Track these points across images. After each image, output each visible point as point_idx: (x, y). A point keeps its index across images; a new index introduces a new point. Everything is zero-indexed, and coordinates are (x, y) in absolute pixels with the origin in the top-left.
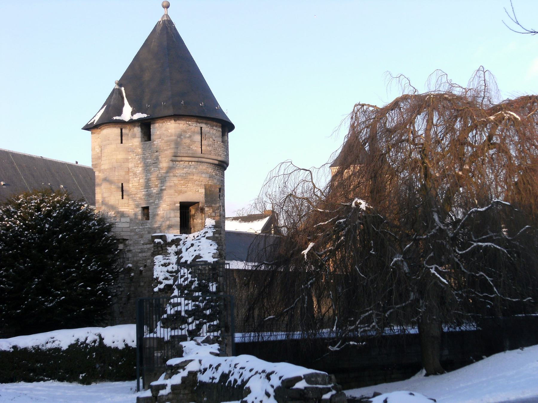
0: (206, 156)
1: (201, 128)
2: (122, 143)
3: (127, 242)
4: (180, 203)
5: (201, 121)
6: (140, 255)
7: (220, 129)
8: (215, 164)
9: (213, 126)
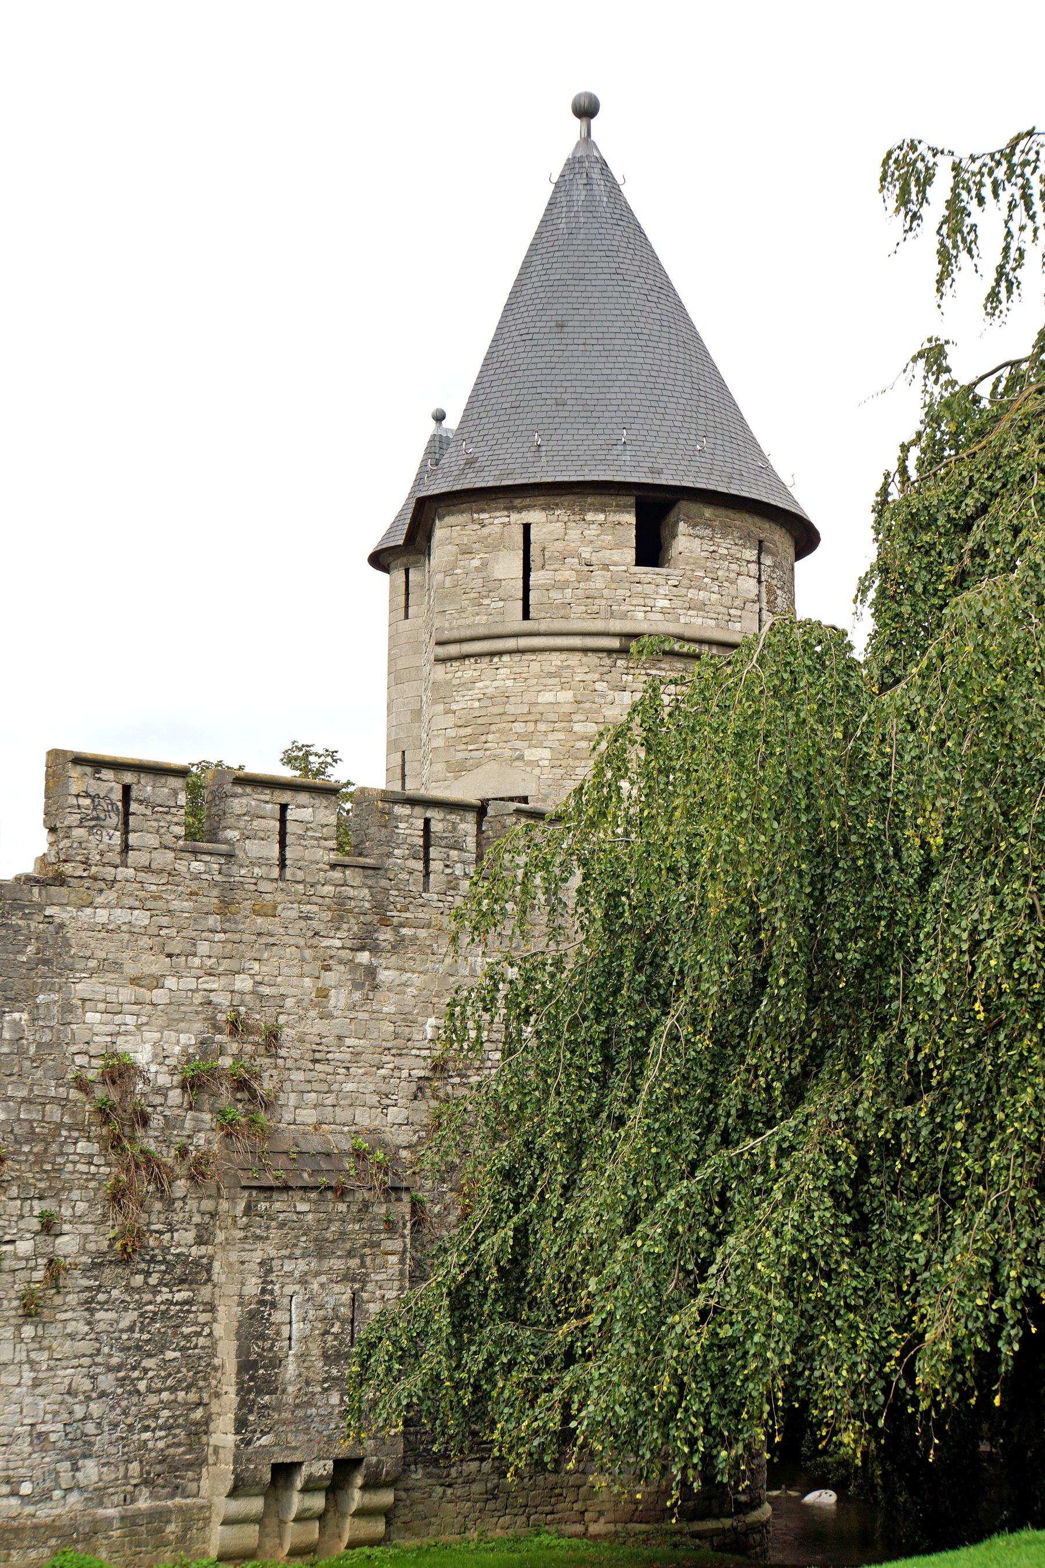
0: (543, 626)
1: (527, 527)
2: (407, 617)
5: (527, 501)
8: (610, 652)
9: (583, 511)
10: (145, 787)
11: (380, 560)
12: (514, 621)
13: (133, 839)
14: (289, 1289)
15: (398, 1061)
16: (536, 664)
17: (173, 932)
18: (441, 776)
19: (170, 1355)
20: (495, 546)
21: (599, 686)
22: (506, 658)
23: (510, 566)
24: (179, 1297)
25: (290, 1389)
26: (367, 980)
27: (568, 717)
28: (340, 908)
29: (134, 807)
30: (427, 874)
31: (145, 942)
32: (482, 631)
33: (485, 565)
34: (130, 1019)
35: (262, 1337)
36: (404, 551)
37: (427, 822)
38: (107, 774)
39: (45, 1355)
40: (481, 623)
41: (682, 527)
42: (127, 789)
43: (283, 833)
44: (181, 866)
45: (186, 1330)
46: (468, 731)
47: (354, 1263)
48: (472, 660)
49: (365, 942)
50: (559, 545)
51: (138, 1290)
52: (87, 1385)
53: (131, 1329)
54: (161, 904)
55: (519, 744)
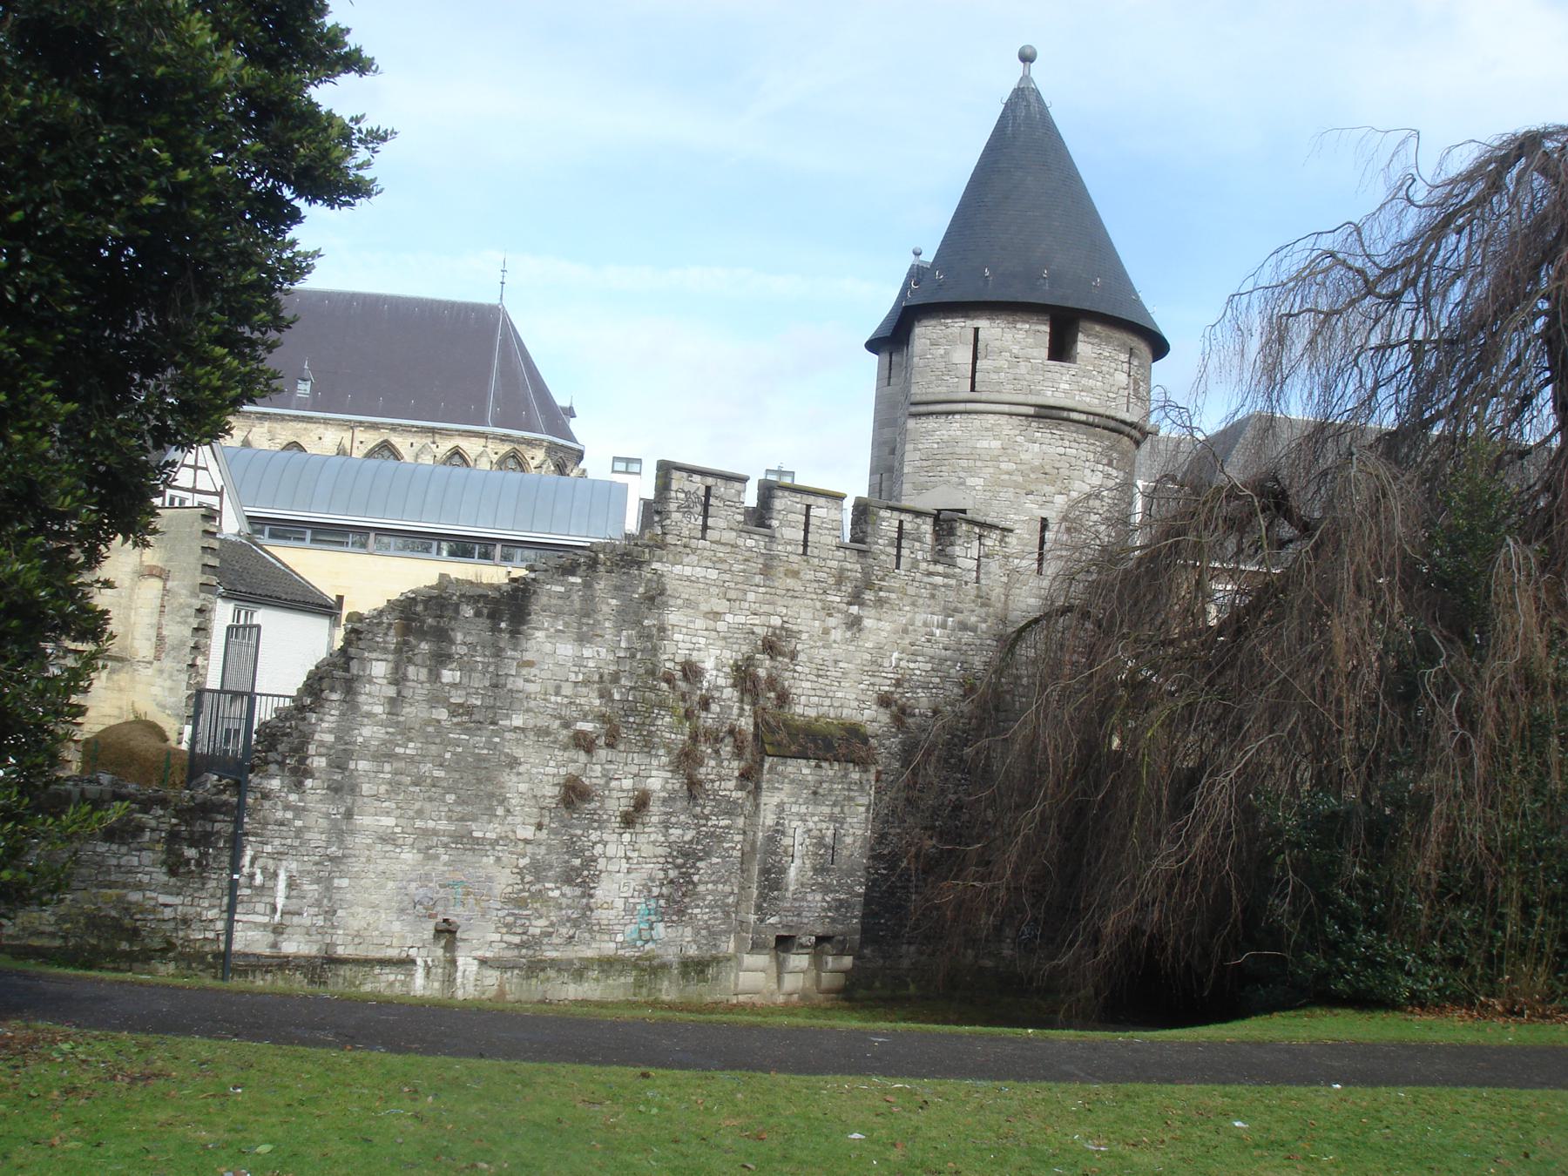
0: (984, 397)
1: (977, 330)
7: (1047, 329)
8: (1027, 416)
9: (1015, 322)
10: (721, 488)
11: (873, 345)
12: (964, 391)
13: (710, 522)
14: (794, 824)
15: (873, 680)
16: (977, 421)
17: (732, 585)
19: (715, 860)
20: (952, 342)
21: (1019, 439)
23: (963, 356)
24: (722, 823)
25: (792, 888)
26: (854, 623)
27: (996, 459)
28: (840, 579)
29: (712, 501)
30: (899, 556)
31: (714, 590)
34: (702, 641)
35: (776, 854)
36: (892, 340)
37: (901, 522)
38: (697, 478)
39: (636, 854)
40: (940, 391)
41: (1081, 336)
42: (708, 489)
43: (807, 524)
44: (740, 542)
45: (726, 845)
47: (837, 810)
49: (856, 598)
50: (998, 343)
51: (695, 816)
52: (661, 875)
53: (691, 842)
54: (726, 567)
55: (962, 474)
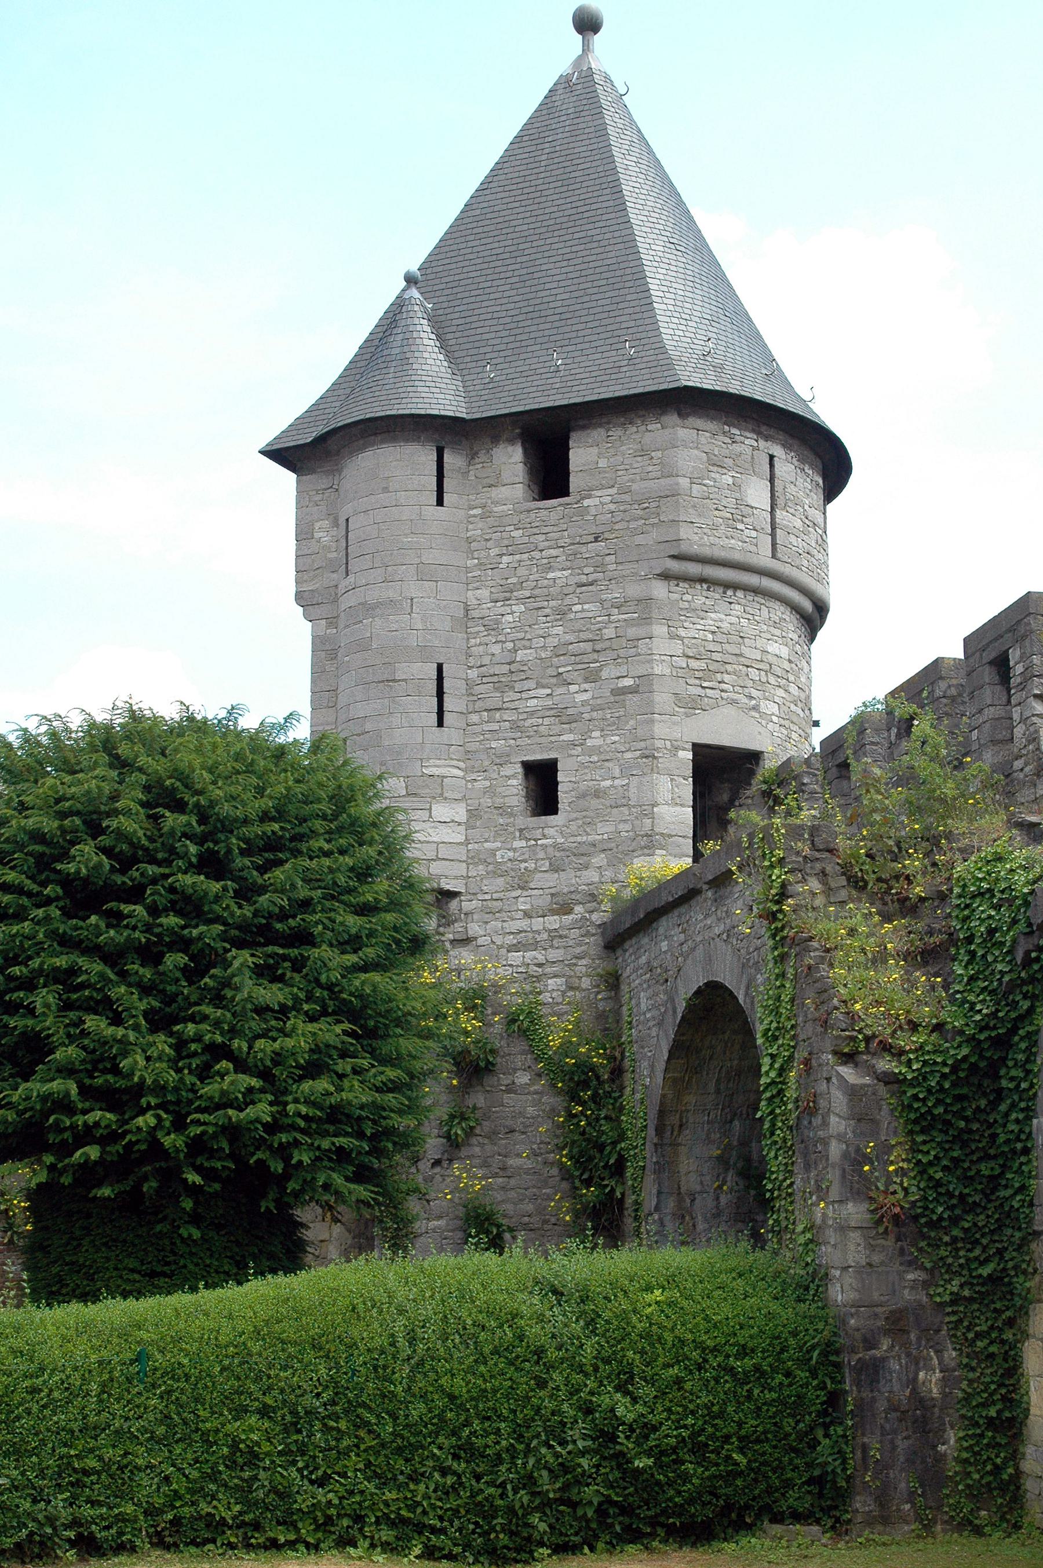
0: (787, 570)
2: (440, 502)
3: (454, 904)
4: (698, 749)
5: (772, 432)
6: (515, 958)
18: (669, 710)
22: (740, 594)
23: (757, 494)
32: (737, 557)
33: (736, 486)
40: (732, 547)
46: (702, 664)
48: (705, 586)
